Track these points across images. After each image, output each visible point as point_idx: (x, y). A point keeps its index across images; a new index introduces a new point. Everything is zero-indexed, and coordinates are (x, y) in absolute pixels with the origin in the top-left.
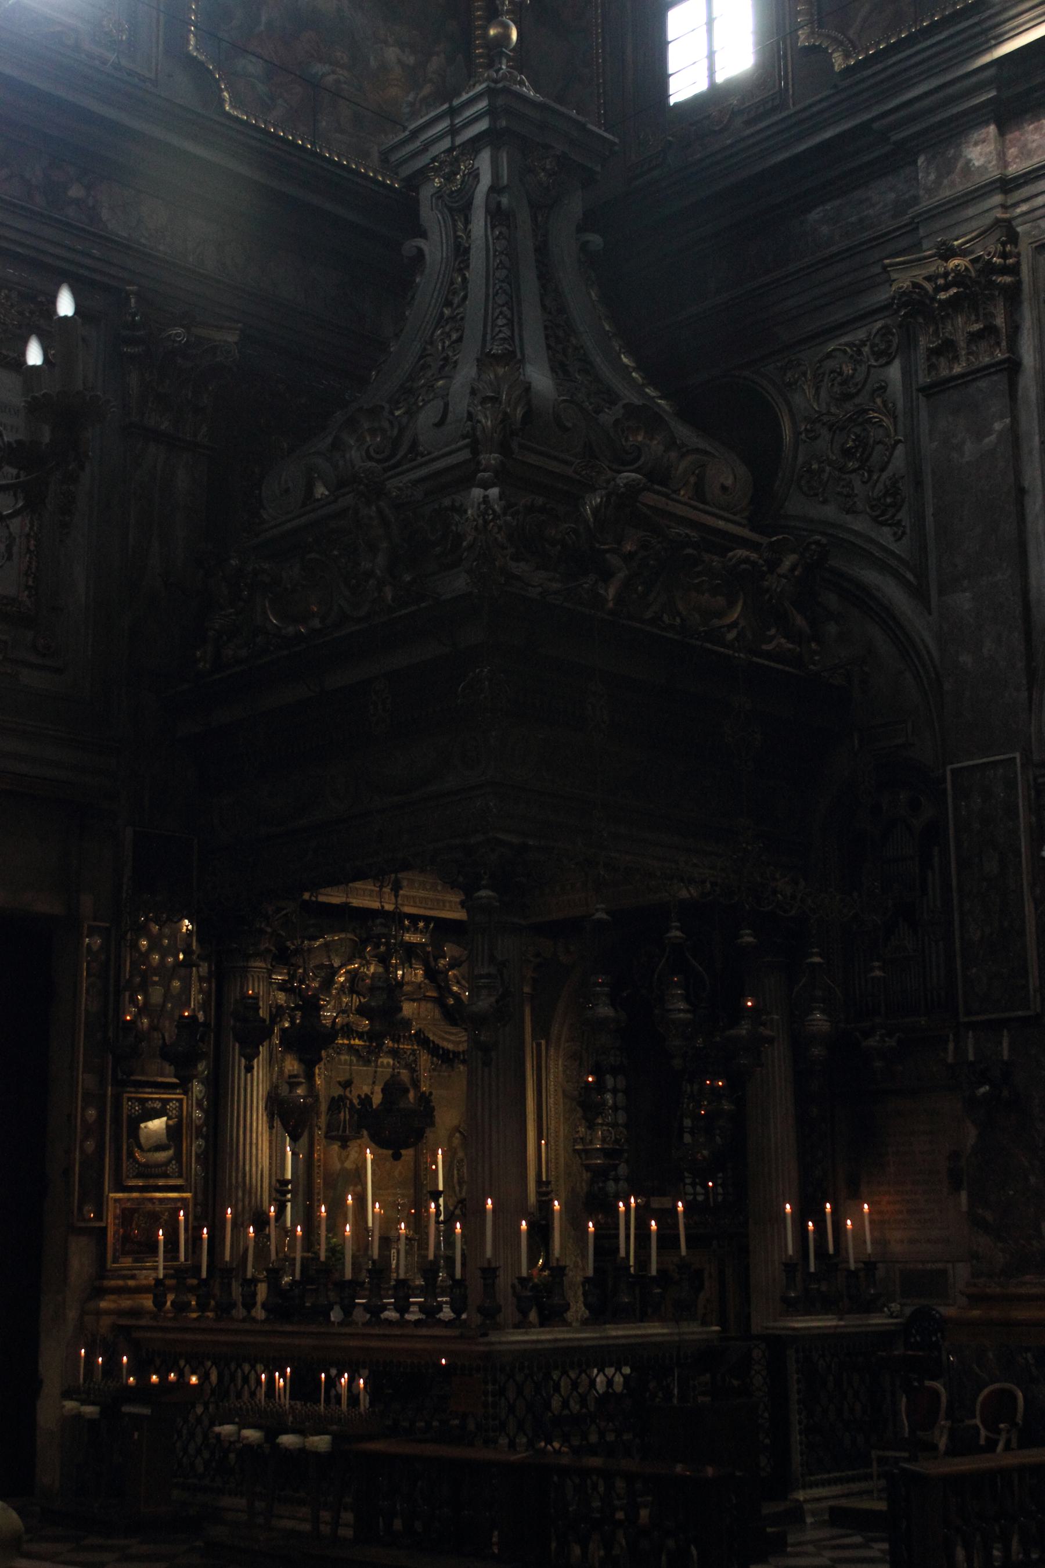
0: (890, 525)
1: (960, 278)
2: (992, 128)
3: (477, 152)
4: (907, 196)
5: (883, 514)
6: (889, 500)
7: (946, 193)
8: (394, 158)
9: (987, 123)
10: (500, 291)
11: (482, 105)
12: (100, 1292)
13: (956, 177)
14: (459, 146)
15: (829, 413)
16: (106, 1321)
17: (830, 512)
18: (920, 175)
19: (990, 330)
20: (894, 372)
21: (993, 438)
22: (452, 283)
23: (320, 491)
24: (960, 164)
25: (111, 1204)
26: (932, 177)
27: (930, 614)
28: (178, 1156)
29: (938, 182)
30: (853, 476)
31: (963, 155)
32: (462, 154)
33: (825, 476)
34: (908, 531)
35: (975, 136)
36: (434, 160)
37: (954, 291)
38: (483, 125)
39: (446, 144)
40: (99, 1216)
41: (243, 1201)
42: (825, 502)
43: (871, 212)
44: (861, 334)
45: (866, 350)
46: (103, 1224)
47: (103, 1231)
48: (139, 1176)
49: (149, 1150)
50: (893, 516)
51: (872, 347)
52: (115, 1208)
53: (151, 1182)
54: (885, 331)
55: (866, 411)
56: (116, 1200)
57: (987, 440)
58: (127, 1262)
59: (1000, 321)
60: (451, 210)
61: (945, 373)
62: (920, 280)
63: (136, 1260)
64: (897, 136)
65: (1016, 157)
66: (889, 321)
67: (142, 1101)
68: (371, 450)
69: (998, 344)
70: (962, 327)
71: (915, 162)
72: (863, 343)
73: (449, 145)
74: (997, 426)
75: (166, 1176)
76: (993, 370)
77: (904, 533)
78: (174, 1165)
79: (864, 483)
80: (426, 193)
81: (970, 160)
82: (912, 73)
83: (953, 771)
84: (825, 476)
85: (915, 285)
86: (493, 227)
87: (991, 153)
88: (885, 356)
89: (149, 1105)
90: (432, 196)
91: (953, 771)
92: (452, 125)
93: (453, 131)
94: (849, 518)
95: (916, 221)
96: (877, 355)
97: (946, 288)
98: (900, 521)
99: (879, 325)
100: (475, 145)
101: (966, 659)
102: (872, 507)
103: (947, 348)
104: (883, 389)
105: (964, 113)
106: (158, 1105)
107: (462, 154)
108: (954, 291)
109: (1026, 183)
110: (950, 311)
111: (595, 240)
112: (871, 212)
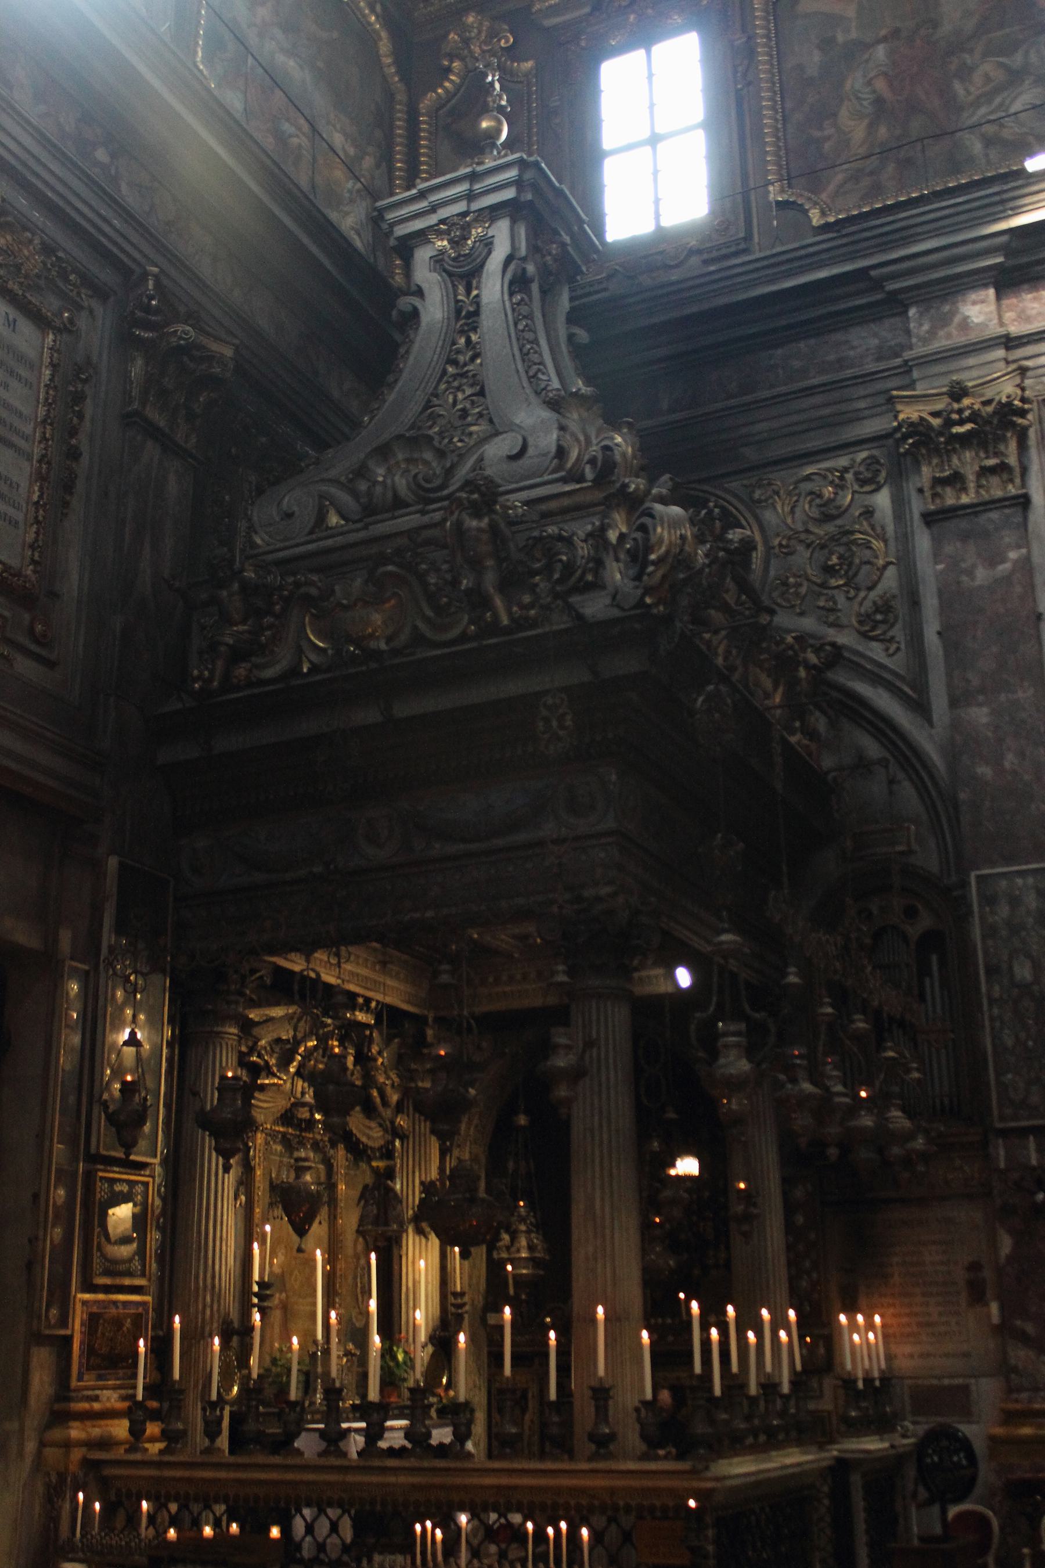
0: (882, 641)
1: (974, 417)
2: (991, 292)
3: (493, 220)
4: (893, 343)
5: (873, 629)
6: (879, 617)
7: (936, 345)
8: (390, 216)
9: (986, 286)
10: (532, 351)
11: (512, 173)
12: (59, 1417)
13: (953, 329)
14: (474, 212)
15: (807, 531)
16: (77, 1454)
17: (808, 624)
18: (912, 325)
19: (1003, 468)
20: (883, 500)
21: (1007, 566)
22: (454, 343)
23: (334, 519)
24: (957, 319)
25: (78, 1306)
26: (926, 327)
27: (931, 724)
28: (141, 1251)
29: (933, 333)
30: (835, 592)
31: (961, 310)
32: (476, 220)
33: (803, 590)
34: (903, 646)
35: (973, 296)
36: (442, 221)
37: (969, 426)
38: (509, 194)
39: (460, 207)
40: (64, 1320)
41: (212, 1307)
42: (802, 614)
43: (852, 353)
44: (843, 462)
45: (849, 476)
46: (69, 1332)
47: (68, 1340)
48: (107, 1273)
49: (115, 1243)
50: (884, 633)
51: (856, 474)
52: (82, 1312)
53: (118, 1281)
54: (872, 461)
55: (852, 533)
56: (85, 1303)
57: (1001, 567)
58: (89, 1380)
59: (1012, 460)
60: (450, 275)
61: (950, 501)
62: (925, 415)
63: (100, 1378)
64: (892, 286)
65: (1014, 320)
66: (875, 452)
67: (112, 1181)
68: (420, 476)
69: (1011, 481)
70: (968, 462)
71: (906, 312)
72: (846, 470)
73: (464, 209)
74: (1013, 555)
75: (130, 1274)
76: (1007, 503)
77: (898, 649)
78: (136, 1264)
79: (849, 599)
80: (423, 255)
81: (968, 317)
82: (919, 230)
83: (978, 877)
84: (803, 590)
85: (922, 419)
86: (511, 294)
87: (991, 312)
88: (869, 482)
89: (118, 1188)
90: (431, 258)
91: (978, 877)
92: (471, 190)
93: (470, 196)
94: (831, 631)
95: (910, 364)
96: (863, 482)
97: (961, 422)
98: (893, 638)
99: (864, 455)
100: (494, 212)
101: (984, 771)
102: (860, 622)
103: (956, 480)
104: (869, 513)
105: (959, 276)
106: (125, 1188)
107: (476, 220)
108: (969, 426)
109: (1028, 343)
110: (957, 446)
111: (583, 336)
112: (852, 353)
